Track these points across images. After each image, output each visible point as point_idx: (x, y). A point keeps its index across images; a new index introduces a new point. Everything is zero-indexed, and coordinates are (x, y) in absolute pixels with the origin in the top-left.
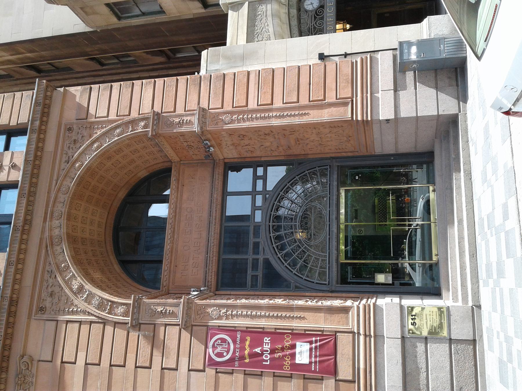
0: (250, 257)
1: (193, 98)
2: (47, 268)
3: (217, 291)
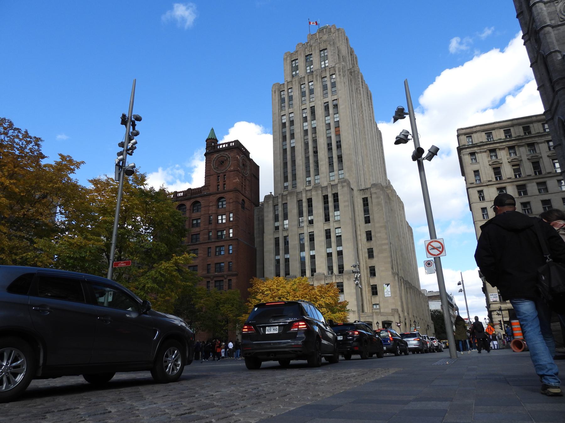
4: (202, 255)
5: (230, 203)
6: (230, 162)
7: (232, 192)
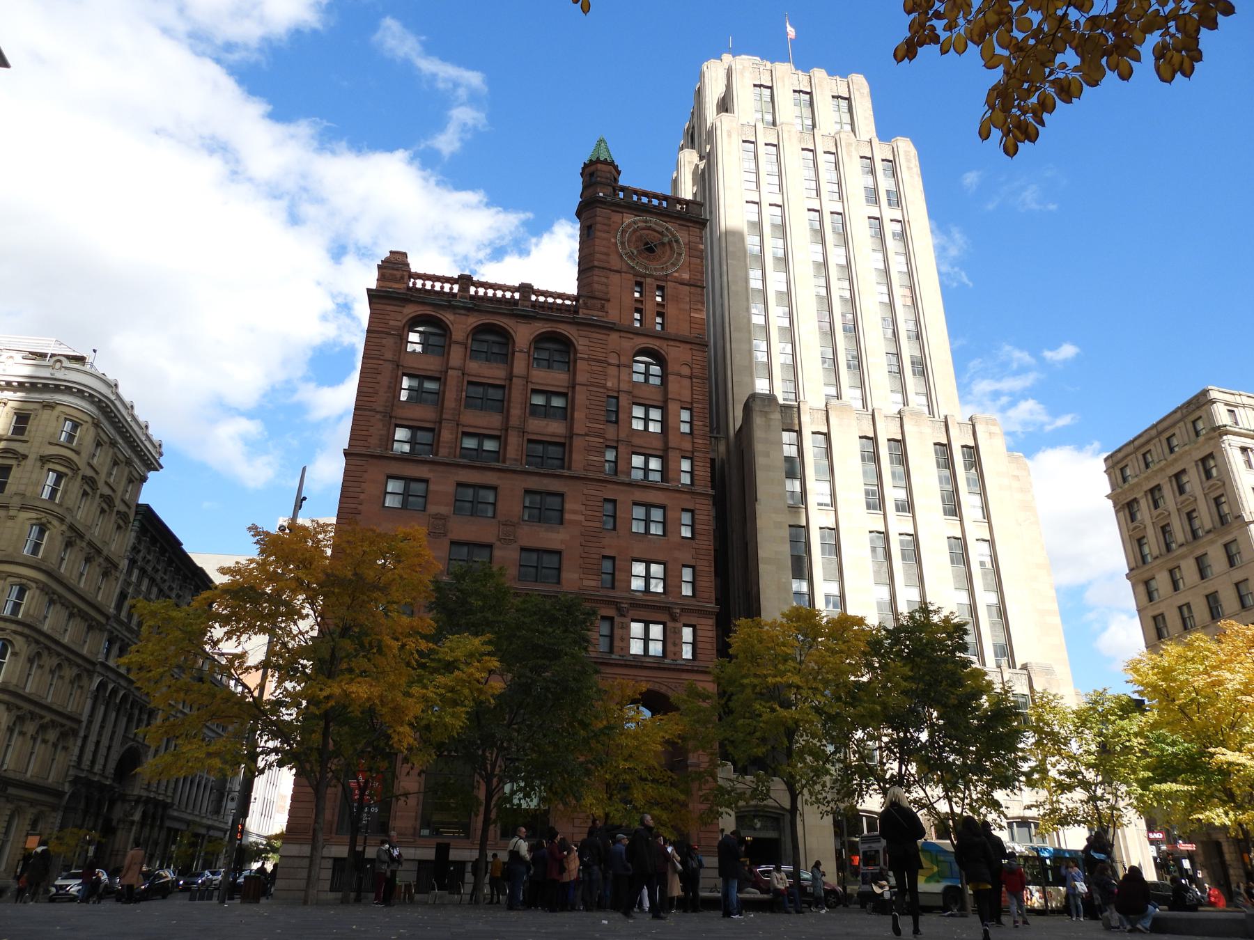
4: (581, 518)
5: (682, 376)
6: (680, 254)
7: (694, 347)
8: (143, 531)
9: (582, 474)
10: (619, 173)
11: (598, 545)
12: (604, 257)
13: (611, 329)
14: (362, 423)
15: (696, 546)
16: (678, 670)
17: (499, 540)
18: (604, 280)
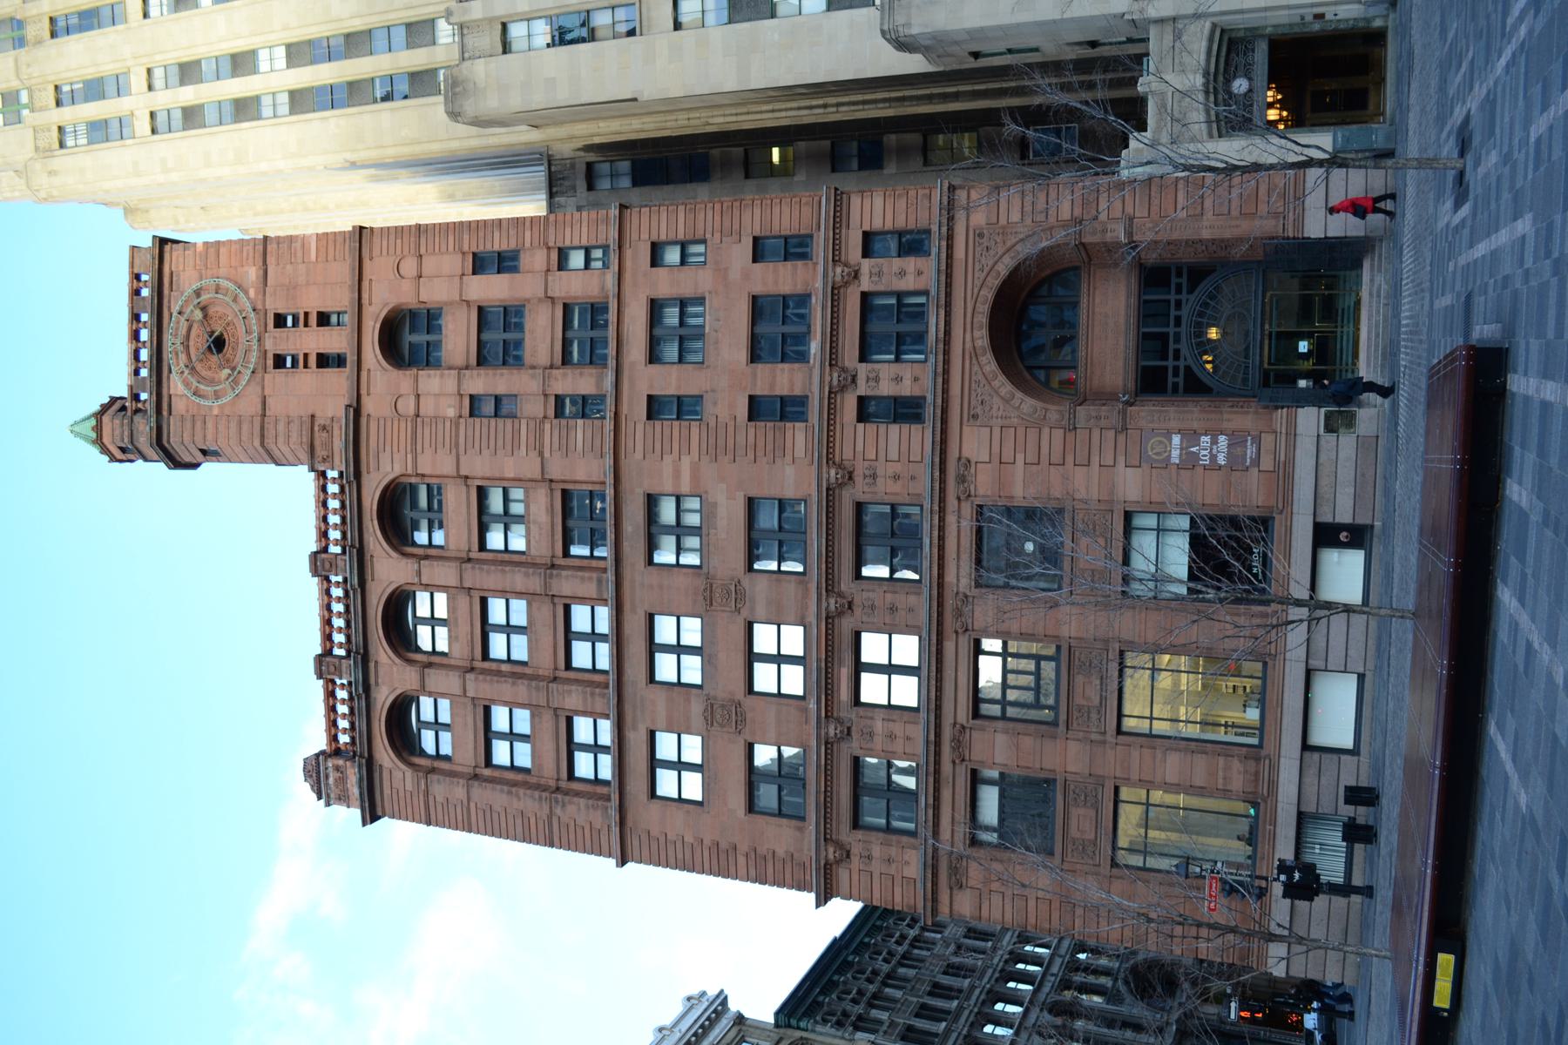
0: (1170, 363)
1: (1118, 205)
2: (974, 378)
3: (1136, 395)
4: (686, 462)
8: (809, 1013)
9: (609, 460)
10: (114, 400)
11: (731, 429)
12: (245, 427)
13: (358, 412)
14: (572, 837)
15: (717, 235)
16: (949, 266)
17: (738, 611)
18: (281, 427)
